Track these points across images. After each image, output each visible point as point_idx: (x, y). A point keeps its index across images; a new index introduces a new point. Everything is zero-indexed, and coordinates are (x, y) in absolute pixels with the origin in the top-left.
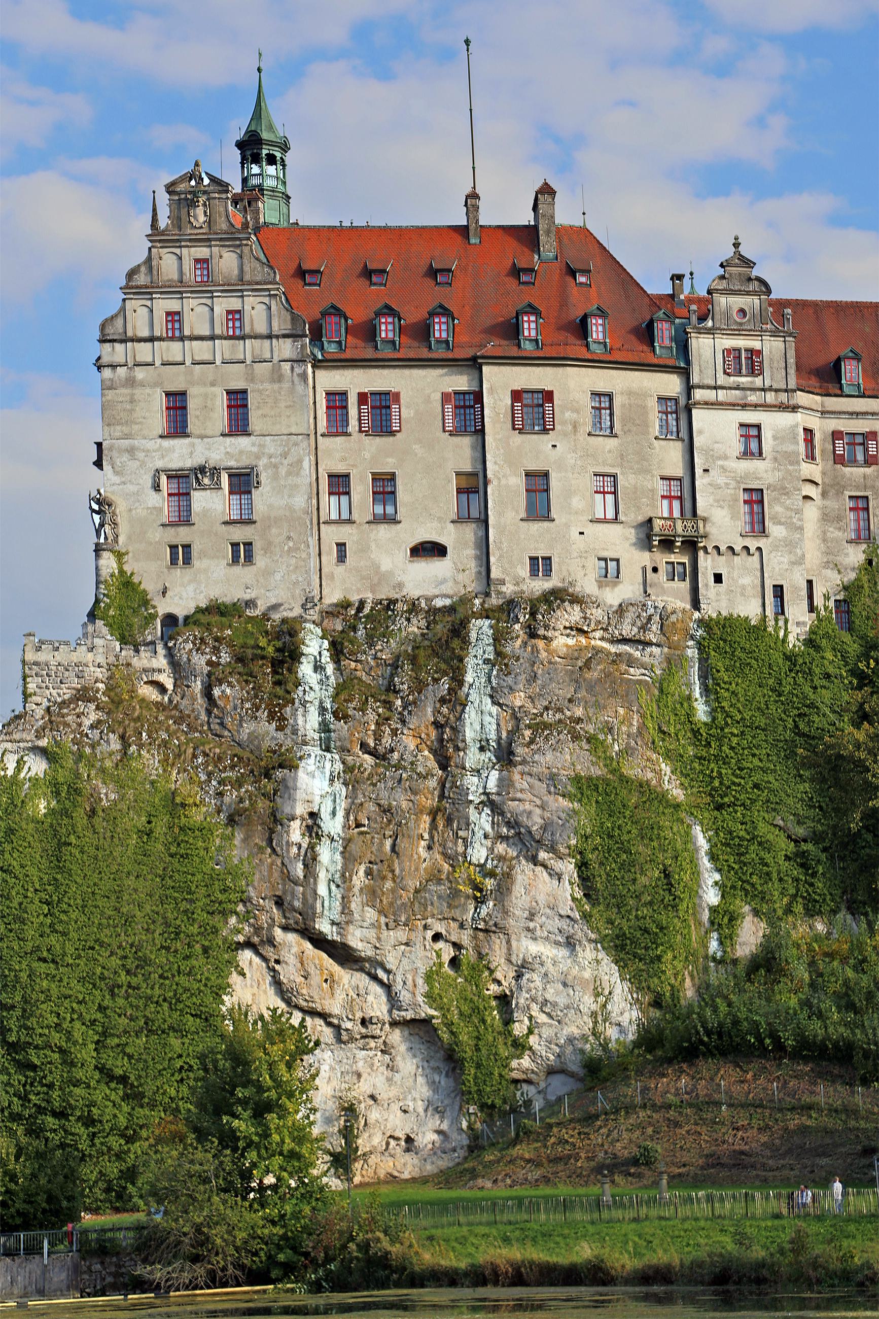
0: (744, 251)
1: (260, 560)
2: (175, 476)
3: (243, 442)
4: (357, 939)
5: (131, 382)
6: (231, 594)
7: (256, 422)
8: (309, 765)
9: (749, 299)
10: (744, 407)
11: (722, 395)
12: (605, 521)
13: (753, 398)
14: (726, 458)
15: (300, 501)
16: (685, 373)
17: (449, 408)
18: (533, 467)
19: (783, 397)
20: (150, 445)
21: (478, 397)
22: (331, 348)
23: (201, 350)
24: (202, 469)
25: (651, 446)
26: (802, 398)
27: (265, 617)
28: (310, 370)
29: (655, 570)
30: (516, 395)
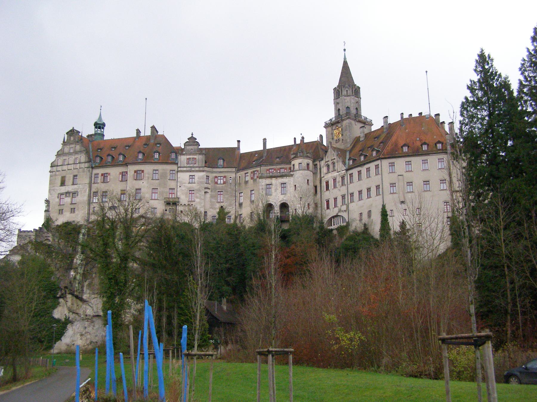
0: (194, 136)
1: (76, 212)
2: (62, 194)
3: (76, 186)
4: (85, 297)
5: (56, 175)
6: (71, 220)
7: (78, 181)
8: (77, 256)
9: (194, 147)
10: (190, 171)
11: (185, 169)
12: (155, 199)
13: (193, 169)
14: (185, 183)
15: (86, 198)
16: (177, 164)
17: (121, 176)
18: (138, 187)
19: (201, 169)
20: (57, 188)
21: (127, 172)
22: (97, 164)
23: (70, 167)
24: (66, 193)
25: (167, 181)
26: (206, 169)
27: (76, 225)
28: (91, 169)
29: (166, 210)
30: (135, 172)
